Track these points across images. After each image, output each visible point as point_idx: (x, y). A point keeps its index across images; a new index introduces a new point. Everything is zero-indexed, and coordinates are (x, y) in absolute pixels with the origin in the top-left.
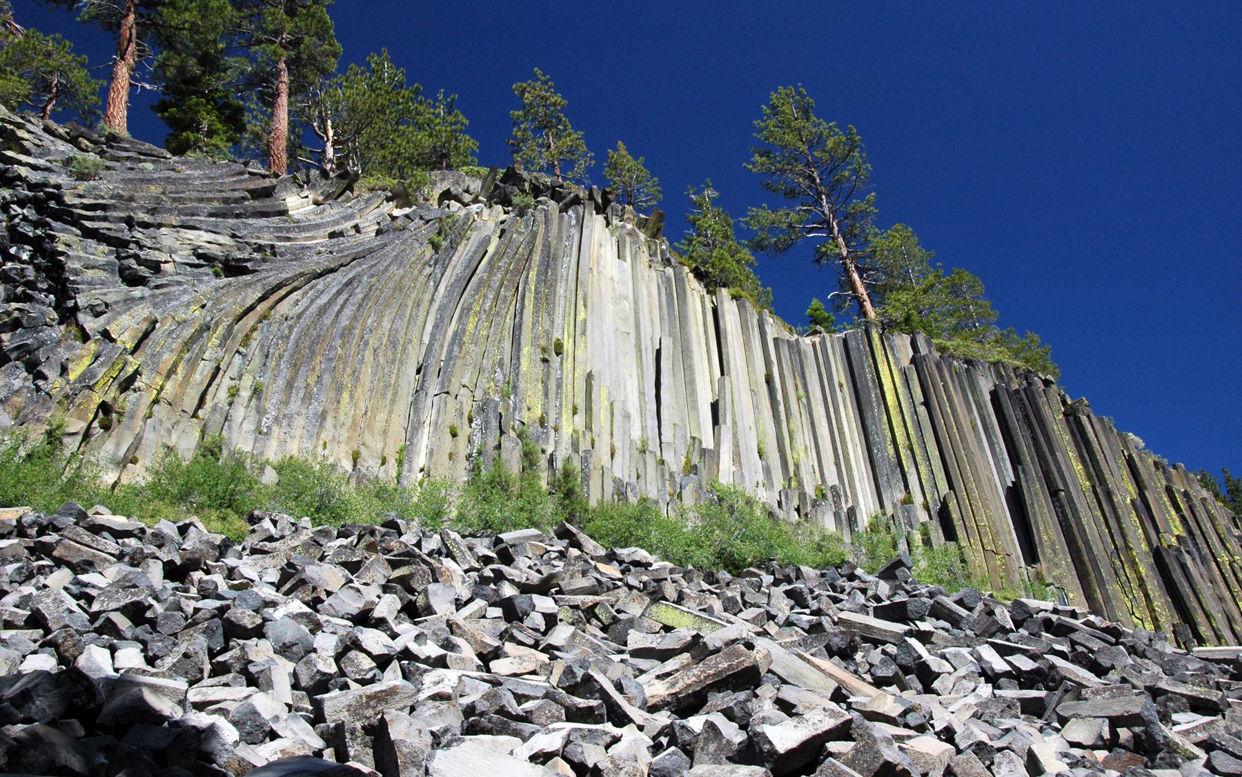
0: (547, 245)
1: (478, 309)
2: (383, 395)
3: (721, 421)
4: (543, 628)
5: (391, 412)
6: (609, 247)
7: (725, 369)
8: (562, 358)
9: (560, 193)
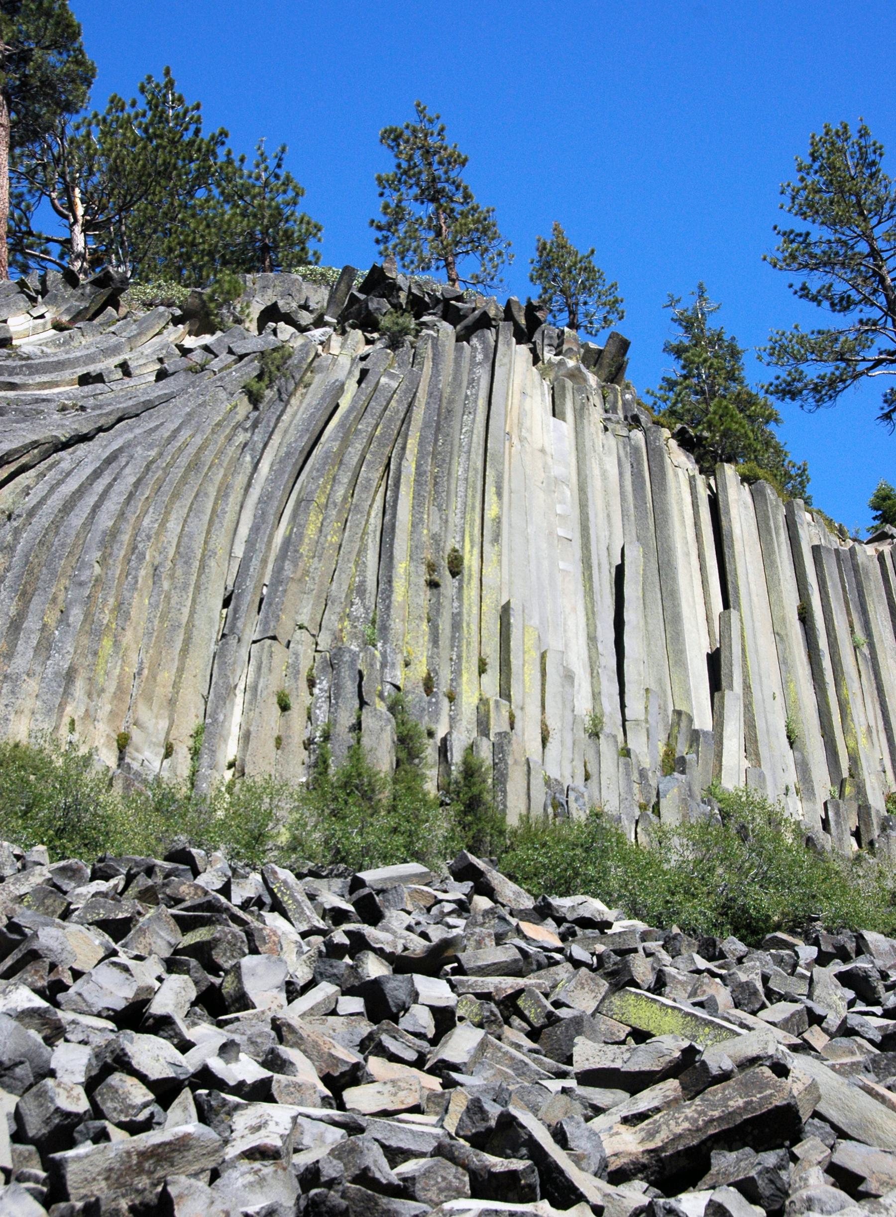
0: (434, 394)
1: (323, 500)
2: (170, 641)
3: (724, 684)
4: (431, 1033)
5: (181, 670)
6: (539, 398)
7: (731, 599)
8: (461, 581)
9: (458, 309)
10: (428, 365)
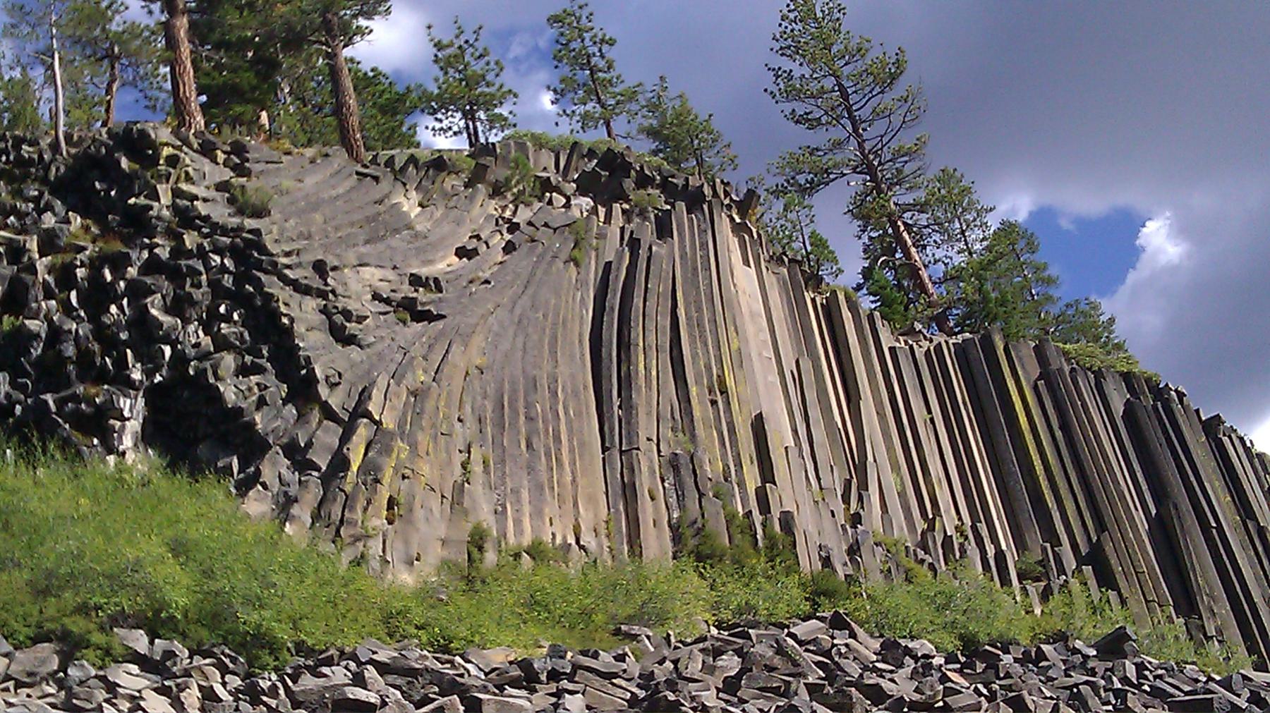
7: (852, 392)
10: (675, 233)
